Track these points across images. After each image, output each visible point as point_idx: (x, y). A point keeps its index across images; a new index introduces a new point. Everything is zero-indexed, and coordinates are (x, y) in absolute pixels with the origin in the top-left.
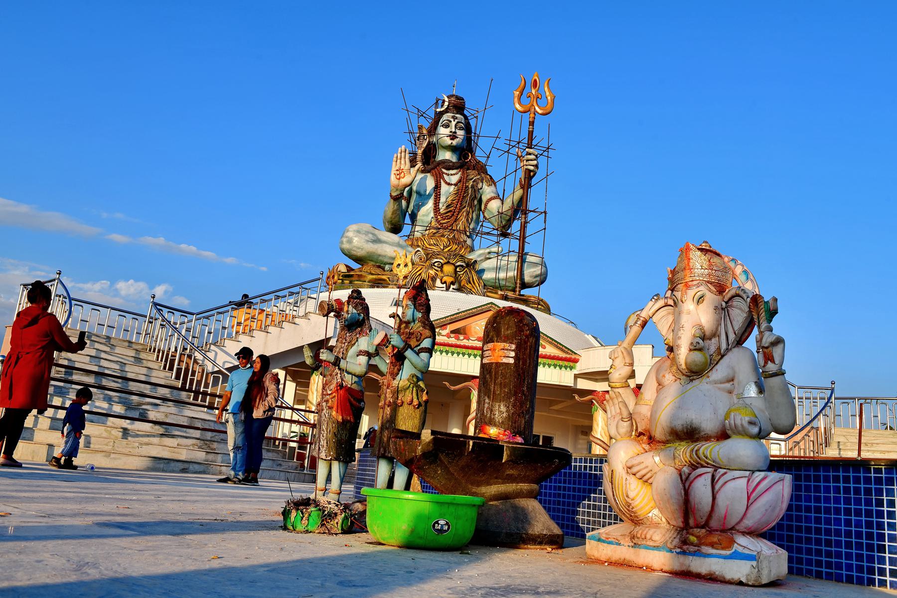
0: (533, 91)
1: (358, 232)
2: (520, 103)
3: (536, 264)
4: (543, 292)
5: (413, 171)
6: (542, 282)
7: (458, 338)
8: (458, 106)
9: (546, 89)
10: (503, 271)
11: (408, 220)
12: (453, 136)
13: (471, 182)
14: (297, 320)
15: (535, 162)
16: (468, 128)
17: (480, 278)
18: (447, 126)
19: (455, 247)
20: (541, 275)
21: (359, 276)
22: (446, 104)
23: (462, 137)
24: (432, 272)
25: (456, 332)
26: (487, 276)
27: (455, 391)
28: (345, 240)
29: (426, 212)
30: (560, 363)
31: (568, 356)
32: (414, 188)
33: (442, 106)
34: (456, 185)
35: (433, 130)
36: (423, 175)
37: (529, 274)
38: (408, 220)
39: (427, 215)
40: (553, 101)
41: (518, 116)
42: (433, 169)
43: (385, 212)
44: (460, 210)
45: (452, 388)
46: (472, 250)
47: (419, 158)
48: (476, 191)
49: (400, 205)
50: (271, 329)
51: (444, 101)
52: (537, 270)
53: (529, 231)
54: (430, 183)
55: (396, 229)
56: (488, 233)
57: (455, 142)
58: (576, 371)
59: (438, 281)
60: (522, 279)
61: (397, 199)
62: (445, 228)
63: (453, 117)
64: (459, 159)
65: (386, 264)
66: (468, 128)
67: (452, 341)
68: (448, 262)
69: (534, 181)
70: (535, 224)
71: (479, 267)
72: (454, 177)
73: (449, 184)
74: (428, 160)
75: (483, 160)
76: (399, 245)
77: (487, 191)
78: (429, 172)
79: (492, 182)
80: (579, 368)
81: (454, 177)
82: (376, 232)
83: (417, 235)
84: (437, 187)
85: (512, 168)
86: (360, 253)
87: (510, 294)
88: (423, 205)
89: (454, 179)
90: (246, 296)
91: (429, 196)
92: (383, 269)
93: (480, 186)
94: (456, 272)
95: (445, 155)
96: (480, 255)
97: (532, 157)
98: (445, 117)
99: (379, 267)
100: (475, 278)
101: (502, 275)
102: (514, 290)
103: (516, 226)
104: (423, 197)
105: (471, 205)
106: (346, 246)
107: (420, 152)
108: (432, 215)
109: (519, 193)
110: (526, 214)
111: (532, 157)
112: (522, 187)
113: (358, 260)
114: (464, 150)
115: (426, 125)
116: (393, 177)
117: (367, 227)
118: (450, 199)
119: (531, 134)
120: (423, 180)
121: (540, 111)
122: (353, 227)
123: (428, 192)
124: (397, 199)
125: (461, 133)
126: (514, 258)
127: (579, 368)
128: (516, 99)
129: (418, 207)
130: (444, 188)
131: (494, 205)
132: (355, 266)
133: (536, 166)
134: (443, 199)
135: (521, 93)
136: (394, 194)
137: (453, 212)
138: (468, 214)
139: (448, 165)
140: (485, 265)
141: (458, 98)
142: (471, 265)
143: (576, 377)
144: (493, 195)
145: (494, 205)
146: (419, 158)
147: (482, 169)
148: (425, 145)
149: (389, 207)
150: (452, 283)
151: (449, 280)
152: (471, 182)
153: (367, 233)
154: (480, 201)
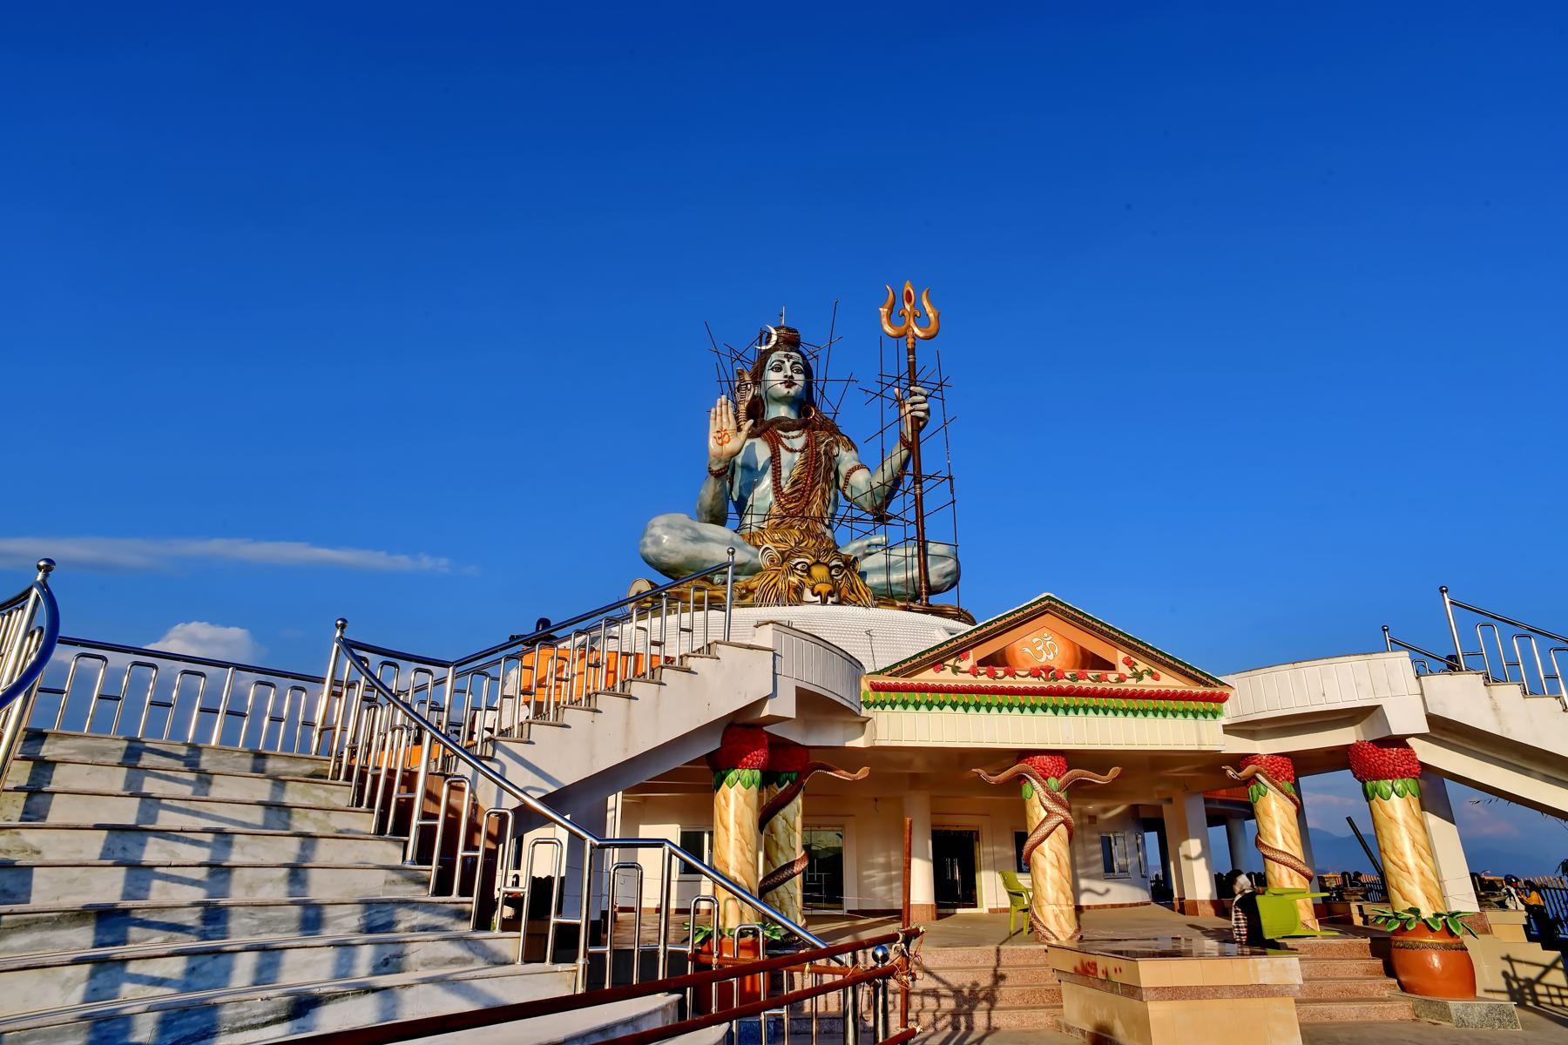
0: (908, 307)
1: (669, 526)
3: (944, 557)
6: (954, 584)
7: (993, 675)
9: (925, 303)
10: (898, 570)
11: (732, 508)
12: (789, 383)
13: (823, 447)
15: (925, 406)
18: (779, 369)
22: (774, 338)
23: (801, 383)
24: (794, 580)
25: (989, 662)
26: (873, 580)
28: (648, 540)
30: (1192, 705)
31: (1209, 690)
32: (739, 460)
33: (767, 343)
34: (801, 451)
35: (758, 377)
37: (937, 571)
40: (938, 318)
42: (764, 431)
44: (812, 488)
48: (831, 458)
49: (723, 485)
50: (637, 688)
51: (770, 335)
52: (949, 565)
57: (792, 391)
58: (1224, 720)
60: (927, 581)
61: (718, 475)
62: (793, 516)
63: (789, 357)
66: (807, 372)
67: (984, 681)
68: (818, 562)
69: (922, 435)
70: (935, 497)
73: (792, 451)
77: (846, 459)
78: (758, 436)
79: (851, 445)
80: (1231, 712)
84: (775, 458)
86: (674, 559)
89: (799, 443)
90: (544, 622)
91: (764, 469)
92: (711, 582)
93: (835, 451)
94: (832, 577)
95: (782, 411)
96: (856, 550)
97: (921, 398)
98: (774, 357)
99: (705, 579)
101: (896, 577)
104: (752, 474)
105: (826, 480)
106: (651, 550)
107: (742, 407)
108: (771, 498)
110: (920, 482)
111: (921, 398)
114: (803, 404)
116: (712, 444)
117: (682, 518)
118: (795, 472)
119: (912, 366)
122: (661, 520)
124: (718, 475)
125: (799, 378)
126: (913, 550)
127: (1231, 712)
128: (884, 320)
129: (750, 486)
130: (785, 456)
132: (662, 580)
133: (927, 411)
134: (785, 473)
136: (715, 468)
138: (823, 494)
140: (865, 564)
141: (789, 330)
142: (850, 564)
145: (860, 478)
147: (833, 430)
148: (749, 398)
150: (830, 594)
151: (824, 588)
152: (823, 447)
153: (683, 527)
154: (837, 473)
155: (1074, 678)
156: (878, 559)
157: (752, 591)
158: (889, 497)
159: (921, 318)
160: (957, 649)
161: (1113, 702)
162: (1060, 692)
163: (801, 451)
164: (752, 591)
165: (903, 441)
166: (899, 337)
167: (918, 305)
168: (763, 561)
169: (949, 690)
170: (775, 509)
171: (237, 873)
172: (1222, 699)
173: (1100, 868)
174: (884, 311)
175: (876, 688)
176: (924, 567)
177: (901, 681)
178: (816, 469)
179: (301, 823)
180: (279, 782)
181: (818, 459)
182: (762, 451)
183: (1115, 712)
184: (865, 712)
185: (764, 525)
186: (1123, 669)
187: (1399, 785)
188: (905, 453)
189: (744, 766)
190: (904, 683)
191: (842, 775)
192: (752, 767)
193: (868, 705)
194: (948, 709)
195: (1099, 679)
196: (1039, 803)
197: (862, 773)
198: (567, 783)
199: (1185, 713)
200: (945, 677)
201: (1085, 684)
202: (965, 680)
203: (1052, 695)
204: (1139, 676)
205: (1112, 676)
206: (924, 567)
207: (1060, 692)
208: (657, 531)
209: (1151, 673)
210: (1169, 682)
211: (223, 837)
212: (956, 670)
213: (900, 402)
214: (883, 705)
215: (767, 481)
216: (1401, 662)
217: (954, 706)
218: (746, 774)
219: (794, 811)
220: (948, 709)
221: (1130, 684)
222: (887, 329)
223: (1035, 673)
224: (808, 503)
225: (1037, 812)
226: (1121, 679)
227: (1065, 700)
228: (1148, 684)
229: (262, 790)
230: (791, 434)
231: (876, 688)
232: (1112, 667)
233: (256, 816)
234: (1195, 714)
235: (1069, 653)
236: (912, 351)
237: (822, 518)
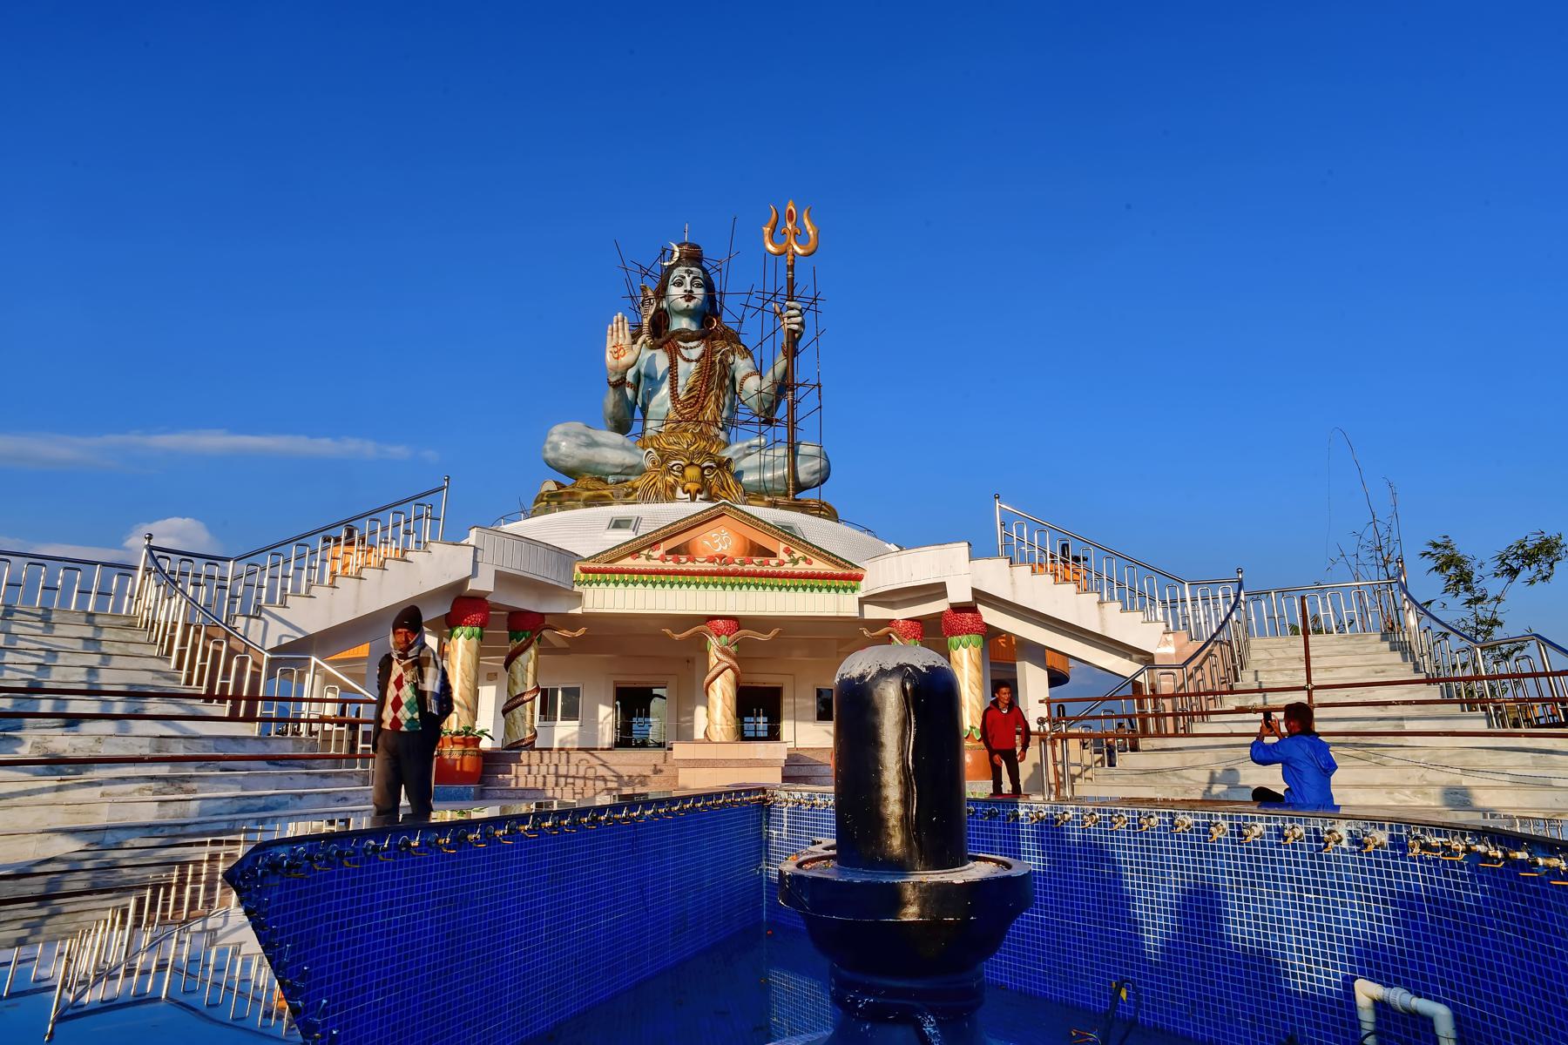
0: (789, 226)
1: (566, 434)
2: (773, 242)
4: (828, 493)
5: (636, 347)
6: (823, 481)
7: (678, 561)
9: (806, 221)
12: (689, 297)
13: (718, 356)
14: (409, 555)
15: (799, 319)
18: (680, 284)
19: (703, 444)
20: (820, 470)
21: (571, 494)
22: (677, 255)
24: (670, 479)
25: (674, 552)
26: (749, 478)
27: (680, 640)
28: (548, 447)
29: (661, 401)
30: (836, 583)
35: (661, 293)
36: (650, 353)
37: (806, 469)
38: (638, 414)
39: (662, 405)
40: (817, 235)
45: (677, 636)
46: (727, 444)
47: (645, 329)
52: (815, 464)
53: (801, 410)
55: (622, 426)
56: (747, 422)
57: (692, 304)
59: (679, 490)
64: (702, 326)
65: (608, 474)
66: (708, 286)
67: (670, 565)
70: (807, 402)
71: (735, 467)
72: (695, 350)
73: (688, 361)
74: (660, 331)
75: (735, 327)
76: (623, 447)
77: (742, 366)
79: (747, 353)
80: (865, 588)
81: (695, 350)
82: (591, 432)
83: (649, 433)
84: (673, 366)
85: (768, 330)
86: (570, 463)
87: (780, 499)
91: (663, 378)
93: (731, 359)
96: (736, 452)
98: (676, 272)
99: (599, 479)
100: (731, 481)
101: (768, 475)
102: (787, 495)
103: (781, 412)
105: (721, 387)
106: (550, 455)
107: (646, 321)
108: (669, 404)
109: (781, 364)
113: (571, 473)
114: (707, 315)
116: (609, 357)
117: (578, 426)
118: (691, 380)
119: (791, 284)
120: (652, 359)
121: (800, 251)
122: (559, 428)
124: (619, 385)
125: (699, 292)
126: (781, 451)
127: (865, 588)
129: (649, 395)
130: (682, 365)
131: (752, 384)
132: (567, 481)
133: (802, 324)
134: (681, 381)
136: (613, 379)
137: (697, 399)
138: (717, 399)
139: (687, 336)
140: (745, 464)
141: (691, 245)
142: (724, 465)
143: (862, 602)
145: (752, 384)
146: (645, 329)
147: (733, 338)
148: (652, 312)
149: (610, 398)
150: (699, 491)
152: (718, 356)
153: (578, 435)
154: (733, 380)
155: (743, 563)
156: (754, 460)
158: (775, 404)
159: (800, 236)
161: (772, 581)
164: (635, 490)
167: (799, 224)
169: (640, 572)
170: (672, 415)
171: (55, 669)
172: (859, 578)
174: (767, 230)
177: (603, 566)
179: (104, 649)
180: (99, 628)
182: (662, 361)
183: (772, 587)
184: (576, 588)
186: (783, 556)
187: (965, 638)
189: (466, 624)
190: (606, 568)
192: (472, 625)
193: (580, 583)
194: (640, 586)
195: (761, 564)
198: (311, 631)
199: (829, 588)
200: (641, 563)
201: (748, 568)
202: (658, 565)
203: (724, 575)
204: (796, 562)
205: (773, 562)
208: (554, 438)
209: (805, 559)
211: (52, 653)
212: (648, 557)
213: (778, 315)
214: (590, 583)
216: (962, 549)
217: (645, 583)
218: (467, 630)
219: (528, 660)
220: (640, 586)
221: (788, 568)
222: (770, 247)
223: (711, 560)
224: (702, 408)
225: (713, 660)
226: (781, 563)
227: (732, 579)
228: (802, 567)
229: (88, 632)
230: (694, 344)
232: (774, 555)
233: (79, 645)
234: (837, 590)
236: (791, 268)
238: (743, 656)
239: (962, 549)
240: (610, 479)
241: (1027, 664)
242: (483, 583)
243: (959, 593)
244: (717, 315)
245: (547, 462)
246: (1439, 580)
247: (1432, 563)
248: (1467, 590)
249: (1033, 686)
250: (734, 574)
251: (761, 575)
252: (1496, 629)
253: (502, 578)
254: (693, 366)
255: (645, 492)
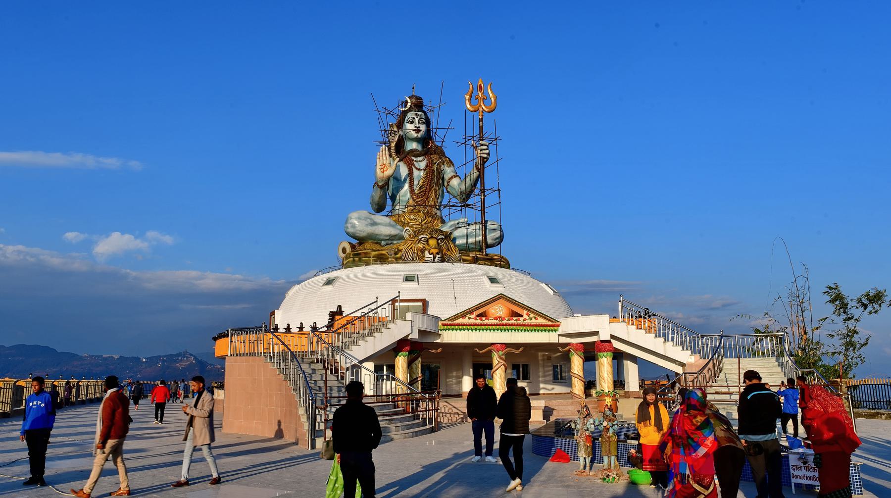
0: (480, 94)
2: (471, 105)
3: (495, 230)
6: (499, 243)
8: (418, 105)
10: (471, 237)
12: (418, 130)
16: (427, 122)
17: (454, 243)
18: (412, 122)
22: (409, 104)
26: (459, 242)
28: (349, 225)
33: (406, 106)
34: (424, 170)
35: (400, 125)
37: (491, 237)
39: (405, 195)
40: (495, 100)
41: (470, 116)
43: (372, 197)
47: (393, 150)
48: (440, 172)
51: (407, 102)
52: (497, 234)
54: (404, 171)
55: (379, 208)
57: (419, 135)
61: (382, 187)
62: (420, 205)
63: (417, 115)
64: (423, 147)
66: (427, 122)
67: (478, 321)
70: (491, 199)
73: (419, 170)
74: (399, 150)
75: (439, 144)
76: (390, 225)
77: (448, 172)
79: (451, 163)
80: (561, 330)
82: (372, 216)
84: (410, 173)
85: (470, 157)
86: (362, 234)
88: (402, 187)
89: (423, 165)
91: (405, 180)
92: (380, 244)
93: (442, 168)
94: (438, 244)
95: (412, 146)
96: (451, 226)
97: (485, 147)
98: (410, 115)
99: (377, 243)
101: (471, 240)
102: (480, 250)
105: (437, 185)
106: (351, 230)
107: (393, 145)
108: (409, 195)
111: (485, 147)
112: (479, 170)
114: (425, 139)
115: (393, 120)
116: (378, 171)
117: (364, 213)
118: (421, 182)
119: (481, 128)
120: (397, 167)
123: (403, 178)
124: (382, 187)
125: (423, 127)
126: (478, 226)
127: (561, 330)
129: (398, 189)
133: (488, 154)
134: (416, 182)
135: (471, 96)
136: (380, 184)
140: (456, 233)
141: (418, 98)
142: (447, 236)
144: (453, 174)
145: (455, 182)
147: (441, 154)
149: (377, 194)
151: (435, 251)
153: (366, 219)
154: (443, 179)
157: (401, 251)
160: (470, 311)
162: (503, 325)
163: (424, 170)
164: (401, 251)
165: (477, 168)
166: (475, 111)
168: (406, 236)
170: (411, 202)
172: (558, 326)
173: (551, 378)
174: (467, 97)
175: (443, 325)
176: (485, 236)
178: (432, 179)
181: (433, 174)
185: (405, 210)
186: (526, 316)
187: (605, 354)
188: (476, 174)
191: (434, 351)
196: (496, 360)
197: (439, 350)
201: (512, 322)
203: (501, 326)
204: (531, 319)
205: (521, 319)
206: (485, 236)
207: (503, 325)
210: (541, 321)
212: (469, 318)
213: (475, 148)
215: (406, 187)
216: (606, 317)
221: (528, 322)
223: (496, 319)
224: (428, 198)
228: (534, 321)
231: (443, 325)
232: (521, 316)
235: (507, 312)
237: (435, 206)
238: (508, 357)
239: (606, 317)
240: (383, 243)
241: (629, 362)
242: (415, 336)
243: (604, 336)
244: (431, 138)
245: (348, 234)
246: (831, 308)
247: (828, 298)
248: (845, 312)
249: (632, 373)
250: (506, 325)
251: (517, 325)
252: (855, 335)
253: (421, 332)
254: (422, 173)
255: (406, 253)
